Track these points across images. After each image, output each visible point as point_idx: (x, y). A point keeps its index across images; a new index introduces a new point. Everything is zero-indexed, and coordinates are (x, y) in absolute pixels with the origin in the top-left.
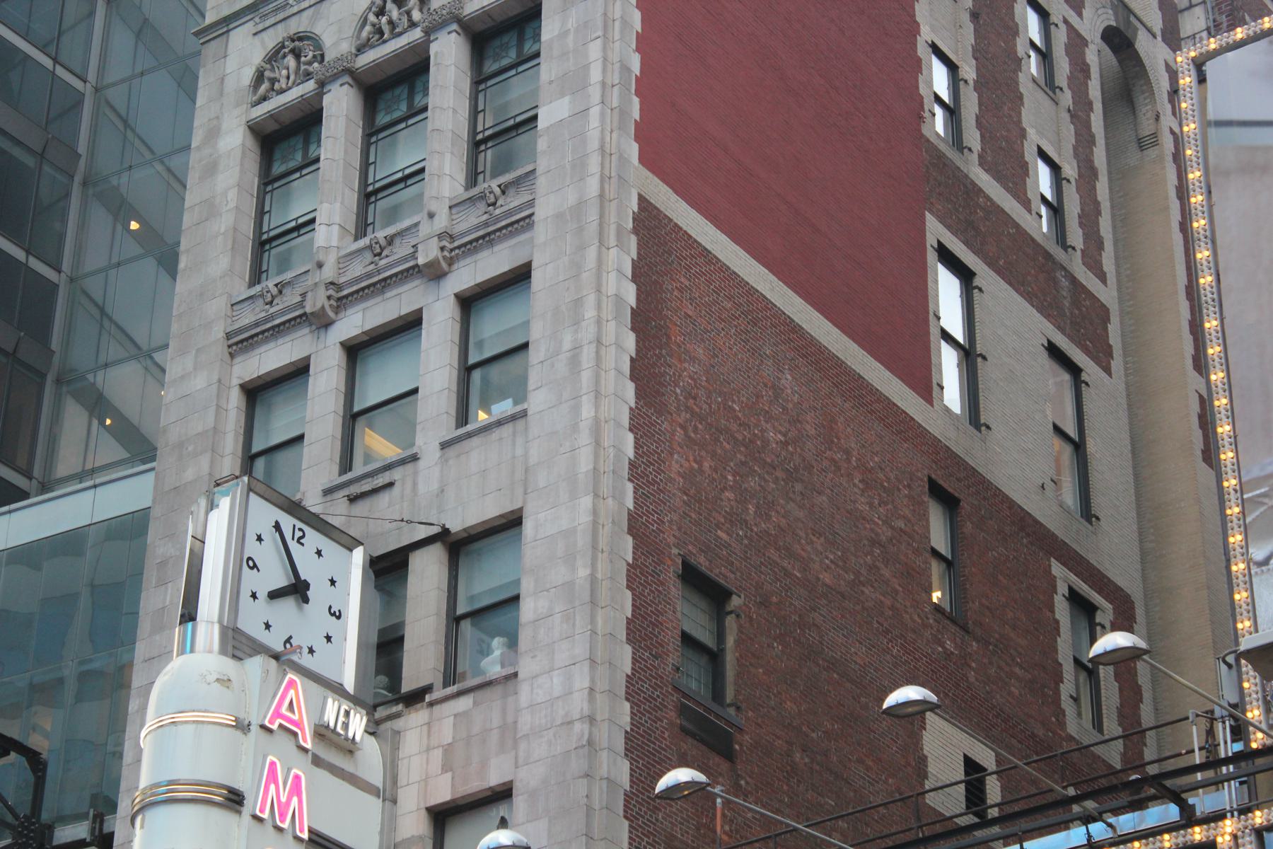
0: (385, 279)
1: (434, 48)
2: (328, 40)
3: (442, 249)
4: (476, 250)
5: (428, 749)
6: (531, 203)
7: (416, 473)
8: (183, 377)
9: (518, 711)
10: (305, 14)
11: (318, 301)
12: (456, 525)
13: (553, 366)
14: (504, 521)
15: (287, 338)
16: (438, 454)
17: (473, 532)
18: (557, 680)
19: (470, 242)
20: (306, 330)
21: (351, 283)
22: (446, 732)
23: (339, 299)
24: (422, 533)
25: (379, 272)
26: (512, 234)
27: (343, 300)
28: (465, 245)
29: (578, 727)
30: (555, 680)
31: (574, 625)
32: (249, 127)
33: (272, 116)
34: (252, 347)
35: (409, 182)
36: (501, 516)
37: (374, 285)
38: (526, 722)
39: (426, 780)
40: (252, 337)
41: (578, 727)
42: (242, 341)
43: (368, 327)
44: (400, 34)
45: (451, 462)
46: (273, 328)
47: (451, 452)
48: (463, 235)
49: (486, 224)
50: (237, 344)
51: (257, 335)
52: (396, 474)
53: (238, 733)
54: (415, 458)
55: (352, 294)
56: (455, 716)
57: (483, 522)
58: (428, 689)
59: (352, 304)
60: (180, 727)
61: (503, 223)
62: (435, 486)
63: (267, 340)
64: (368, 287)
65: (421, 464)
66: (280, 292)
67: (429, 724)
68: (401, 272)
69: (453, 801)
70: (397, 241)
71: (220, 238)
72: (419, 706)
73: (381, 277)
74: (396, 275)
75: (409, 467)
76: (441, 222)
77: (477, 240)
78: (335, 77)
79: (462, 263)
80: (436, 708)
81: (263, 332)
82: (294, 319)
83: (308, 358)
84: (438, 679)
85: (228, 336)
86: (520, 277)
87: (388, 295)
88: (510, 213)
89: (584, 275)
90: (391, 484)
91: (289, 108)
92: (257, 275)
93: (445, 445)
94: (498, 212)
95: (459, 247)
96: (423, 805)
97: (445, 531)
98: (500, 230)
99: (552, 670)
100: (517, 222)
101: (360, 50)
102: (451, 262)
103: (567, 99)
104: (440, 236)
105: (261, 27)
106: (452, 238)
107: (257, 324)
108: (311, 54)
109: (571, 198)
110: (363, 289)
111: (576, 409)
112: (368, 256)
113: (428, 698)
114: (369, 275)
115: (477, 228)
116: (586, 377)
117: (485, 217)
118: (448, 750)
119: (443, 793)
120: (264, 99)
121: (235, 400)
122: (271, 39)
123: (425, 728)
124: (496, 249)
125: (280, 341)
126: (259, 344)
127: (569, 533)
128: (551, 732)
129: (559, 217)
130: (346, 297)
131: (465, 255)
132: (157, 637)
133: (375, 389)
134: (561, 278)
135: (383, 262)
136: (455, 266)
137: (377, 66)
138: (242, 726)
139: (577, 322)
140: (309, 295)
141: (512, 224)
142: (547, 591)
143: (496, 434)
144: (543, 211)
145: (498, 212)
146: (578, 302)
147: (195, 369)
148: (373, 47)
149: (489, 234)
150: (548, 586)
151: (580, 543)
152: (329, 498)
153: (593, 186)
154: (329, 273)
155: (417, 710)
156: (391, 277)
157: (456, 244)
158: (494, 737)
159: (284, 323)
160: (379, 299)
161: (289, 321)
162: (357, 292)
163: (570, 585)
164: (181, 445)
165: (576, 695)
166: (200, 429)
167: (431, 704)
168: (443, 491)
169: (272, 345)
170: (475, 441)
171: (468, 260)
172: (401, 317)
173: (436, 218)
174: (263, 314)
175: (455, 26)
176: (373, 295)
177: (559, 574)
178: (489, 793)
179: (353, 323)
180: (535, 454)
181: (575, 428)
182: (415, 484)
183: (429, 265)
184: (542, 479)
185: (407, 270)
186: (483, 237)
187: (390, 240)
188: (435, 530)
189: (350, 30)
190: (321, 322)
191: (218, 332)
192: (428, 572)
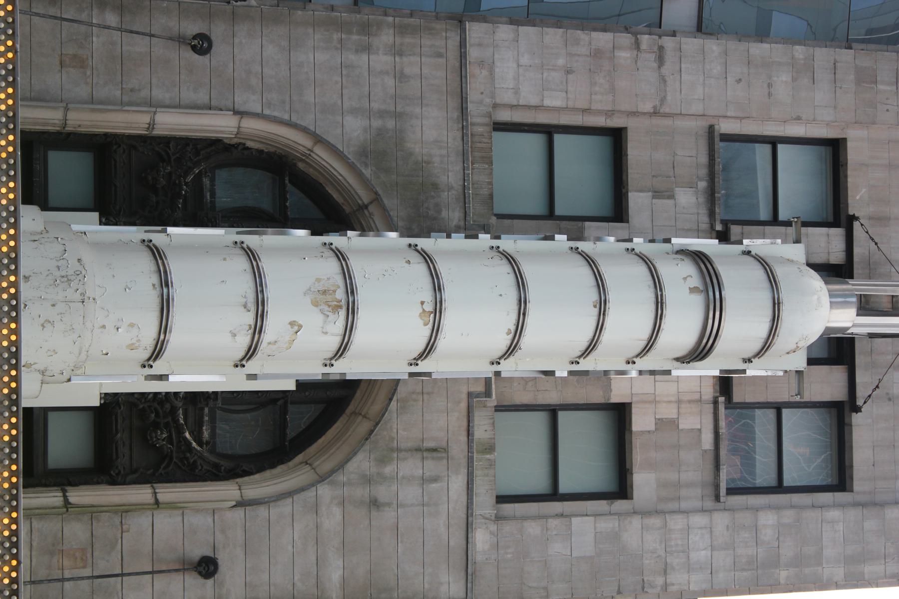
5: (679, 402)
14: (847, 463)
17: (846, 428)
18: (700, 555)
22: (687, 423)
29: (660, 581)
30: (703, 553)
31: (743, 570)
36: (851, 466)
38: (677, 523)
39: (655, 402)
56: (700, 430)
57: (851, 447)
67: (700, 401)
69: (631, 431)
72: (718, 388)
80: (709, 408)
96: (634, 399)
97: (857, 409)
99: (713, 548)
113: (722, 399)
118: (673, 424)
119: (640, 422)
123: (697, 396)
128: (662, 553)
132: (852, 77)
142: (778, 538)
150: (781, 539)
151: (807, 571)
155: (714, 386)
158: (672, 476)
165: (686, 576)
167: (715, 402)
168: (890, 399)
177: (788, 550)
178: (628, 467)
184: (871, 524)
188: (860, 402)
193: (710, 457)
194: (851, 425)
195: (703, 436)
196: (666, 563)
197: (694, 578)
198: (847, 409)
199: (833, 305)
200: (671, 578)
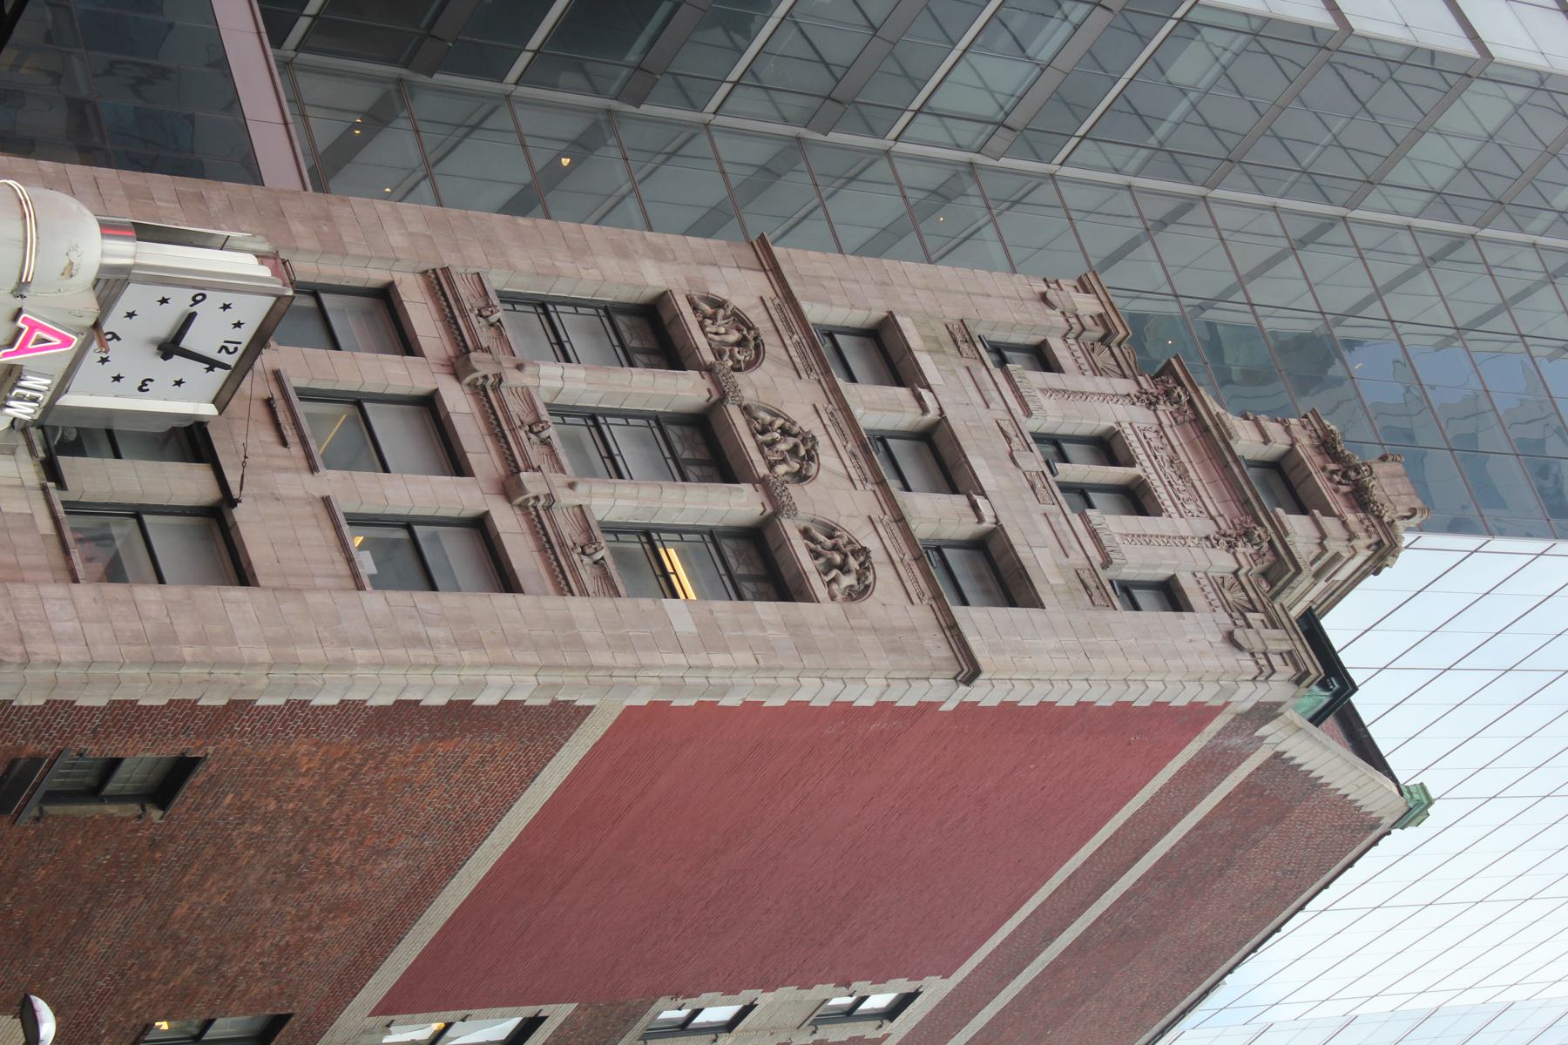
0: (505, 437)
1: (746, 488)
2: (755, 375)
3: (537, 498)
4: (535, 533)
6: (584, 592)
7: (297, 470)
8: (402, 221)
9: (36, 583)
10: (782, 351)
11: (482, 365)
12: (240, 514)
13: (411, 617)
14: (244, 565)
15: (442, 332)
16: (318, 494)
17: (232, 533)
18: (71, 626)
19: (543, 528)
20: (451, 352)
21: (501, 401)
22: (16, 505)
23: (484, 388)
24: (232, 478)
25: (512, 430)
26: (551, 572)
27: (480, 392)
28: (541, 522)
32: (665, 293)
33: (677, 317)
34: (433, 295)
35: (608, 461)
36: (249, 563)
37: (499, 425)
38: (23, 592)
40: (444, 295)
41: (18, 649)
42: (440, 284)
43: (454, 418)
44: (762, 452)
45: (309, 508)
46: (454, 317)
47: (320, 509)
48: (551, 519)
49: (562, 544)
50: (437, 278)
51: (447, 300)
52: (296, 449)
53: (13, 285)
54: (313, 469)
55: (489, 401)
58: (61, 485)
59: (478, 402)
60: (19, 223)
61: (563, 563)
62: (283, 491)
63: (441, 310)
64: (497, 419)
65: (307, 476)
66: (492, 325)
68: (512, 455)
70: (545, 450)
71: (548, 262)
73: (507, 433)
74: (509, 448)
75: (304, 464)
76: (566, 498)
77: (546, 534)
78: (716, 383)
79: (521, 519)
81: (449, 306)
82: (463, 340)
83: (422, 355)
84: (72, 495)
85: (446, 270)
86: (506, 581)
87: (488, 439)
88: (574, 569)
89: (508, 650)
90: (284, 443)
91: (685, 333)
92: (511, 299)
93: (326, 501)
94: (576, 557)
95: (538, 516)
98: (557, 559)
100: (565, 578)
101: (746, 410)
102: (523, 507)
103: (694, 630)
104: (550, 496)
105: (769, 304)
106: (548, 508)
107: (457, 300)
108: (741, 358)
109: (590, 635)
110: (494, 413)
111: (364, 643)
112: (529, 419)
113: (51, 485)
114: (509, 420)
115: (558, 535)
116: (399, 653)
117: (570, 544)
120: (695, 309)
121: (376, 276)
122: (756, 316)
123: (18, 482)
124: (536, 555)
125: (439, 325)
126: (436, 302)
127: (232, 640)
128: (12, 620)
129: (570, 622)
130: (486, 395)
131: (530, 522)
132: (121, 192)
133: (389, 426)
134: (505, 626)
135: (523, 434)
136: (518, 511)
137: (729, 427)
138: (21, 288)
139: (458, 643)
140: (487, 356)
141: (562, 572)
143: (339, 557)
144: (575, 604)
145: (576, 557)
146: (479, 644)
147: (410, 234)
148: (749, 423)
149: (552, 547)
151: (218, 649)
152: (270, 377)
153: (602, 658)
154: (513, 378)
156: (507, 443)
157: (542, 513)
159: (459, 329)
160: (484, 430)
161: (461, 334)
162: (492, 407)
163: (174, 639)
164: (329, 218)
166: (345, 239)
167: (44, 489)
169: (436, 316)
170: (331, 534)
171: (525, 526)
172: (464, 453)
173: (568, 491)
174: (468, 307)
175: (769, 510)
176: (488, 424)
177: (185, 626)
179: (458, 402)
180: (315, 599)
181: (345, 642)
182: (285, 469)
183: (520, 484)
184: (289, 606)
185: (514, 461)
186: (549, 541)
187: (546, 442)
190: (458, 366)
191: (449, 259)
192: (187, 483)
193: (55, 541)
194: (235, 523)
195: (38, 521)
196: (21, 633)
197: (63, 648)
198: (225, 509)
199: (103, 236)
200: (31, 648)
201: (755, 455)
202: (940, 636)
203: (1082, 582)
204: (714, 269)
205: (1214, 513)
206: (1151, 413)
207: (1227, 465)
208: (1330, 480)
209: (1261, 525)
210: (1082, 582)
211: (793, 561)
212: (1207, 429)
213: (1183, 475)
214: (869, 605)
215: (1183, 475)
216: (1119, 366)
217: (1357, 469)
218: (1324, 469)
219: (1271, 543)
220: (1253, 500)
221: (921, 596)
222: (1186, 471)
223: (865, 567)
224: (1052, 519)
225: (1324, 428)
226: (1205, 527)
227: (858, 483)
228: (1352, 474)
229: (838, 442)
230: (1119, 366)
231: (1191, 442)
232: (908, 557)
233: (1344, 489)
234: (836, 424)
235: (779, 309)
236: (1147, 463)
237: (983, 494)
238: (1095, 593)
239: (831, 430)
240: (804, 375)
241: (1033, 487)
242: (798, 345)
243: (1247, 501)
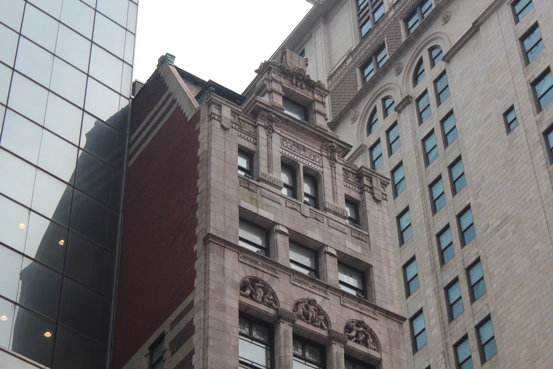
10: (265, 275)
78: (287, 320)
105: (243, 260)
122: (252, 273)
189: (293, 303)
201: (318, 330)
202: (390, 320)
203: (356, 238)
204: (226, 270)
205: (319, 152)
206: (275, 133)
207: (303, 128)
208: (297, 86)
209: (332, 142)
210: (356, 238)
211: (362, 353)
212: (287, 121)
213: (304, 149)
214: (382, 338)
215: (304, 149)
216: (249, 124)
217: (301, 75)
218: (293, 84)
219: (340, 146)
220: (322, 135)
221: (375, 314)
222: (304, 147)
223: (366, 327)
224: (332, 226)
225: (278, 67)
226: (326, 163)
227: (327, 296)
228: (301, 78)
229: (309, 289)
230: (249, 124)
231: (288, 130)
232: (356, 303)
233: (304, 86)
234: (300, 282)
235: (245, 258)
236: (304, 161)
237: (324, 245)
238: (360, 237)
239: (303, 286)
240: (278, 276)
241: (317, 219)
242: (264, 266)
243: (319, 136)
